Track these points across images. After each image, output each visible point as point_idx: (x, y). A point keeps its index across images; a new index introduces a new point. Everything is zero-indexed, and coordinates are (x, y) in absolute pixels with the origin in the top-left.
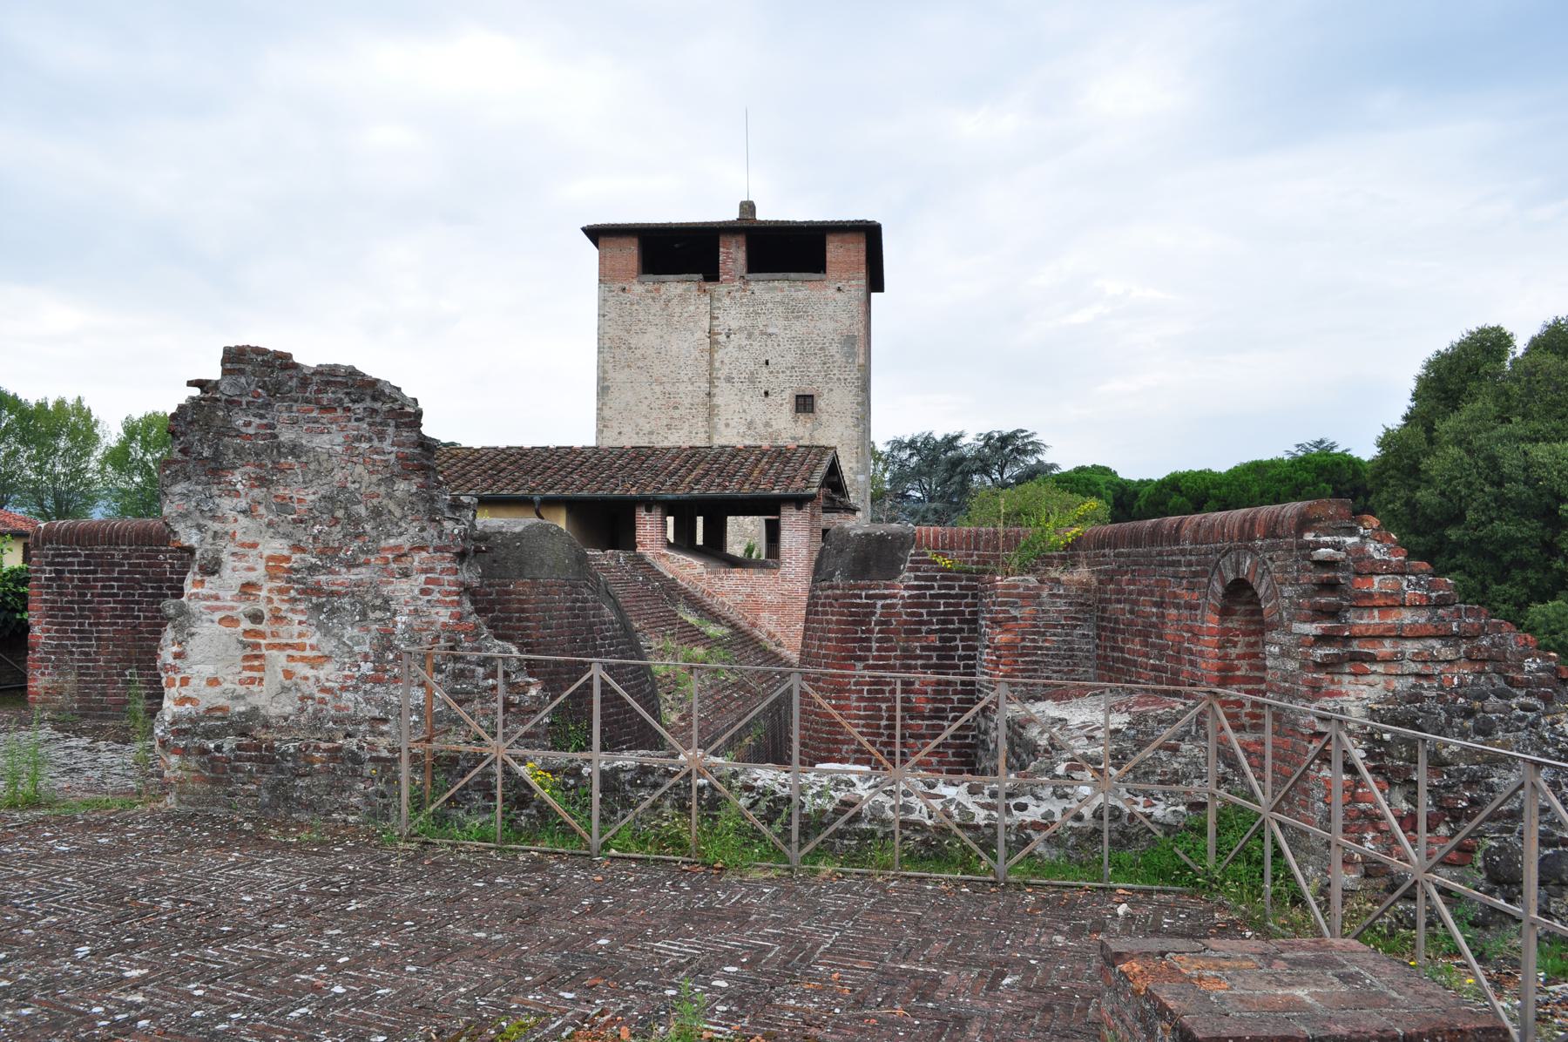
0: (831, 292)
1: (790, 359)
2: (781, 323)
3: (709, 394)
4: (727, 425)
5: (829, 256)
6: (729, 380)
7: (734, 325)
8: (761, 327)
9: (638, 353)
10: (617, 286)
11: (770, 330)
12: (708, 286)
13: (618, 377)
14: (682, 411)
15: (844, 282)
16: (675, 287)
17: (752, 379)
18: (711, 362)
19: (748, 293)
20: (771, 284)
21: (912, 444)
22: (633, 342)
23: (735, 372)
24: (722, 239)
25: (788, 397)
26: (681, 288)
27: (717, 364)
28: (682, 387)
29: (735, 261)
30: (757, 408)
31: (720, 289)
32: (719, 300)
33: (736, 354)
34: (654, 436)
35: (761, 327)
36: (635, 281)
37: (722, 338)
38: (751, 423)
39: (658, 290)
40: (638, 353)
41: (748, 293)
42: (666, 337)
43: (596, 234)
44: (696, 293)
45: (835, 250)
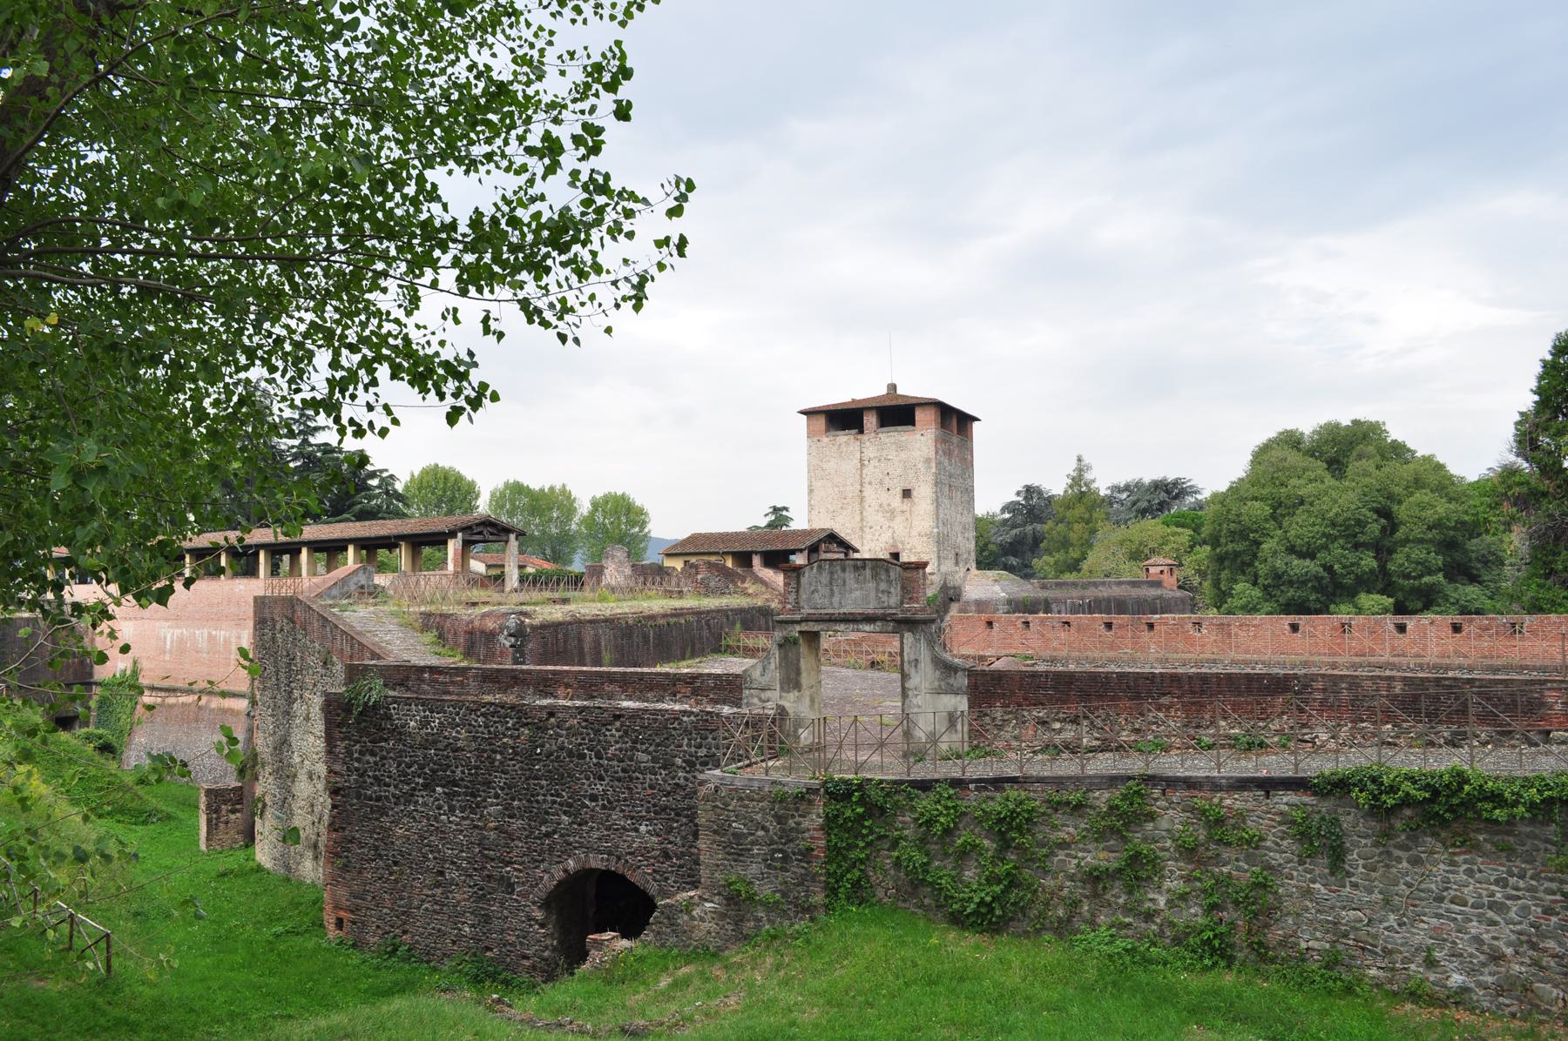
0: (918, 436)
1: (899, 471)
6: (870, 483)
10: (815, 439)
12: (859, 436)
13: (818, 484)
16: (845, 438)
17: (881, 483)
21: (1127, 488)
22: (824, 466)
25: (898, 492)
26: (845, 438)
30: (884, 497)
31: (865, 438)
43: (803, 413)
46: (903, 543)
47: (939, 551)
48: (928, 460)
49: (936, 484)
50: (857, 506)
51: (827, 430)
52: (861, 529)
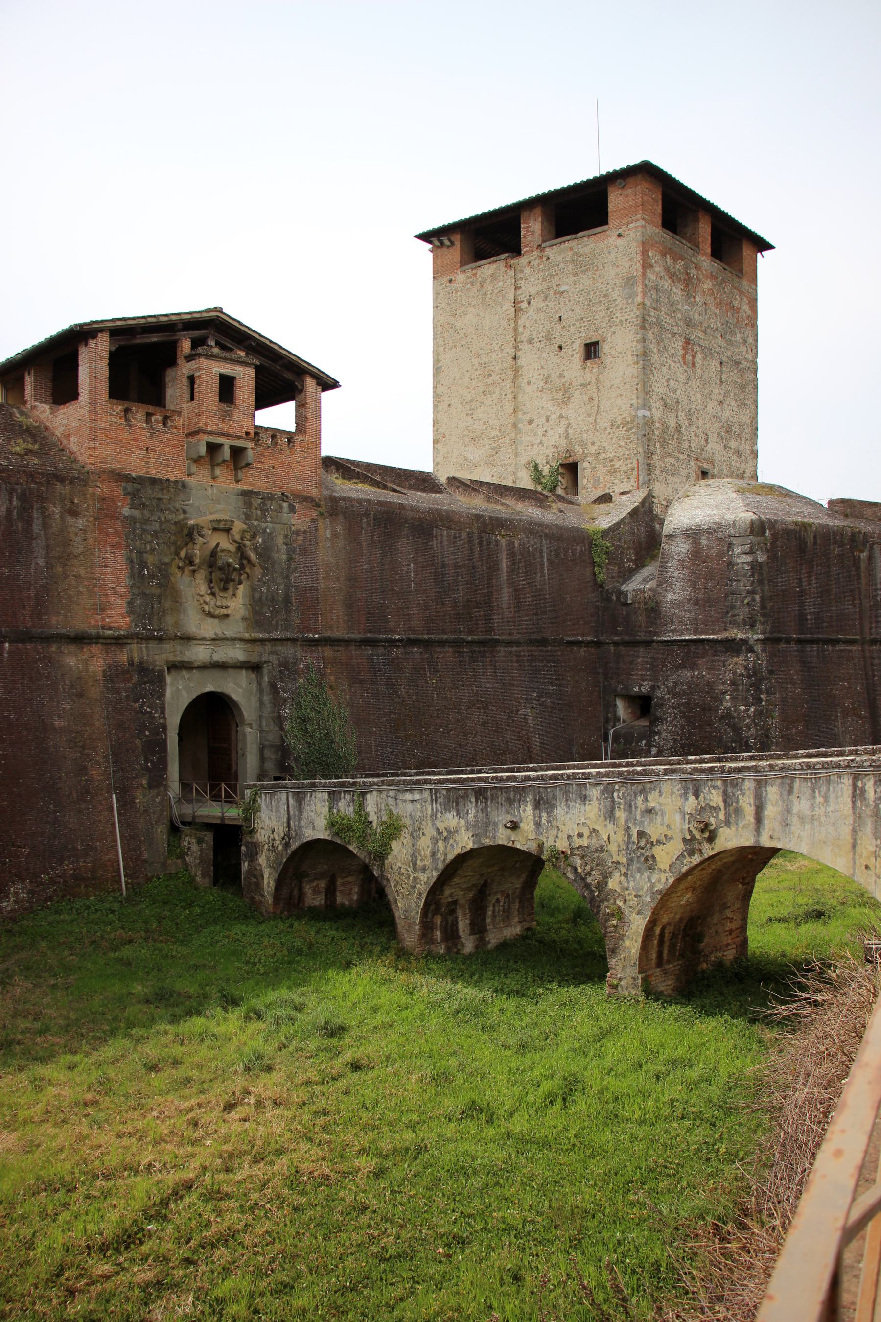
0: (613, 240)
2: (571, 279)
3: (515, 358)
4: (529, 383)
5: (611, 207)
6: (530, 341)
7: (533, 291)
8: (555, 288)
9: (462, 333)
10: (447, 278)
11: (563, 288)
12: (513, 262)
14: (495, 377)
15: (624, 228)
16: (488, 269)
18: (516, 330)
19: (544, 259)
20: (563, 246)
22: (458, 325)
23: (534, 333)
24: (524, 216)
26: (493, 267)
27: (521, 329)
28: (494, 356)
29: (533, 233)
31: (523, 260)
32: (522, 271)
33: (535, 317)
34: (474, 404)
35: (555, 288)
36: (459, 272)
37: (524, 305)
38: (549, 376)
39: (475, 275)
40: (462, 333)
41: (544, 259)
42: (481, 313)
43: (425, 237)
44: (504, 269)
45: (616, 200)
46: (584, 446)
47: (649, 455)
48: (629, 282)
49: (644, 325)
50: (508, 384)
51: (463, 263)
52: (515, 425)
